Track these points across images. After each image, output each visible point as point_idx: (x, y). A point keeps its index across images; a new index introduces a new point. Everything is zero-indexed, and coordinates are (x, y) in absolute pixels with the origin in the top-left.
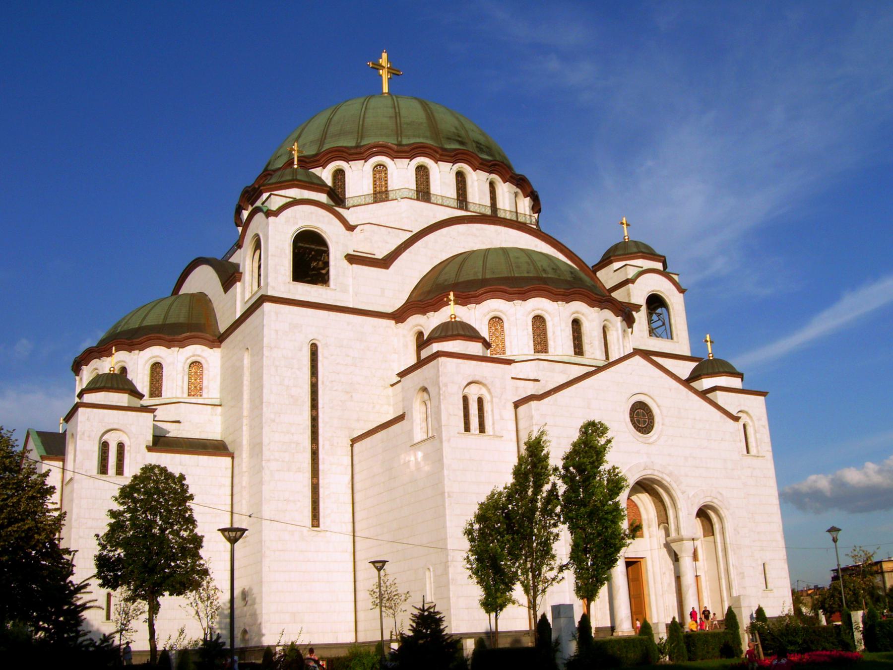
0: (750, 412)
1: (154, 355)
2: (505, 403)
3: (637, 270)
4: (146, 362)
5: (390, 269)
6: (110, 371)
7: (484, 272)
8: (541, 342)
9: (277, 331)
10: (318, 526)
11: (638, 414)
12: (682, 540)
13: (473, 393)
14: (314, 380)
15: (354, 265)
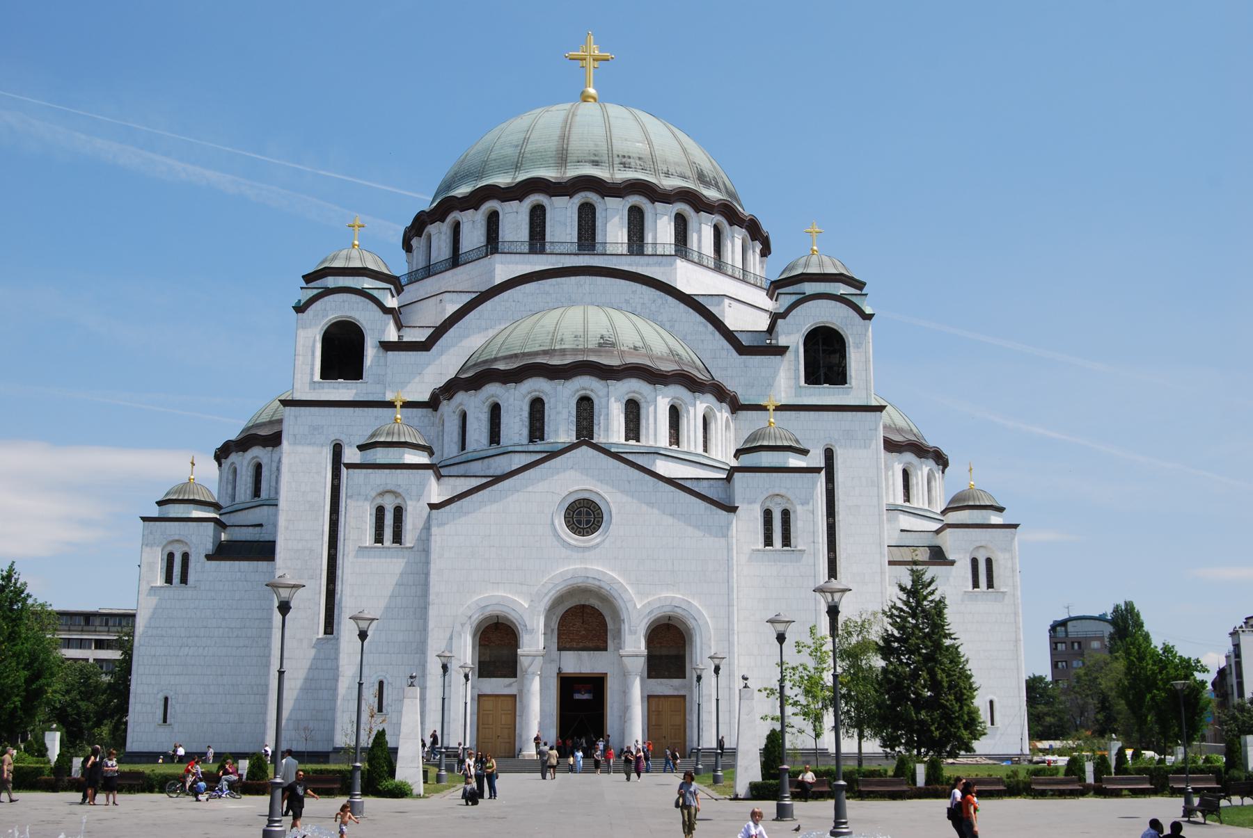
0: (789, 495)
1: (255, 455)
2: (421, 511)
3: (794, 298)
4: (249, 464)
5: (431, 351)
6: (190, 480)
7: (499, 350)
8: (537, 428)
9: (295, 435)
10: (332, 633)
11: (580, 513)
12: (622, 657)
13: (389, 504)
14: (336, 482)
15: (389, 352)
